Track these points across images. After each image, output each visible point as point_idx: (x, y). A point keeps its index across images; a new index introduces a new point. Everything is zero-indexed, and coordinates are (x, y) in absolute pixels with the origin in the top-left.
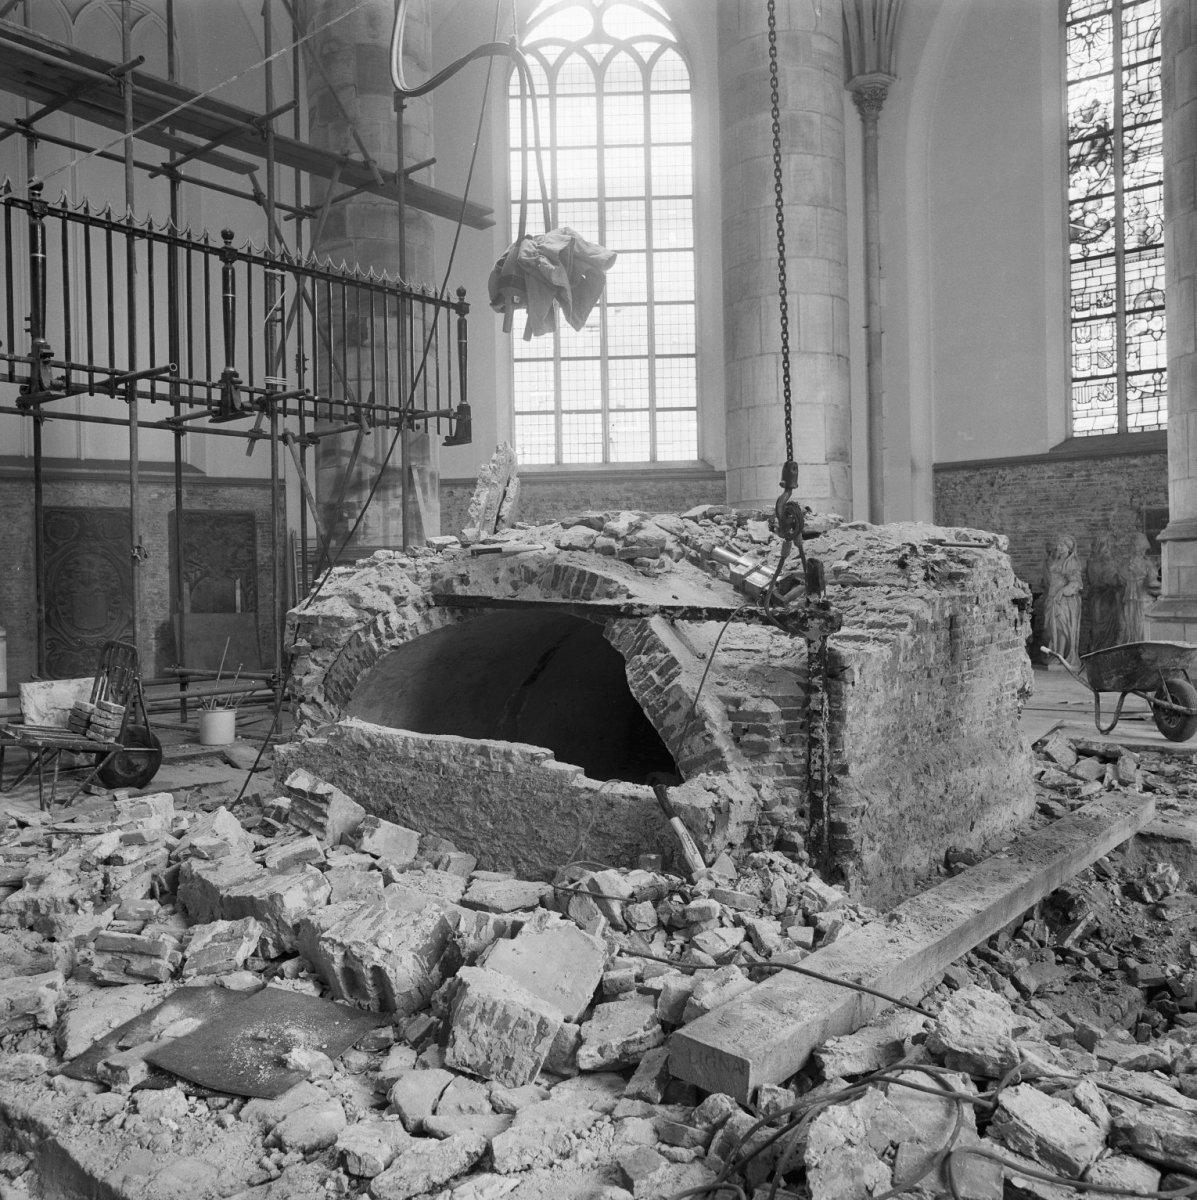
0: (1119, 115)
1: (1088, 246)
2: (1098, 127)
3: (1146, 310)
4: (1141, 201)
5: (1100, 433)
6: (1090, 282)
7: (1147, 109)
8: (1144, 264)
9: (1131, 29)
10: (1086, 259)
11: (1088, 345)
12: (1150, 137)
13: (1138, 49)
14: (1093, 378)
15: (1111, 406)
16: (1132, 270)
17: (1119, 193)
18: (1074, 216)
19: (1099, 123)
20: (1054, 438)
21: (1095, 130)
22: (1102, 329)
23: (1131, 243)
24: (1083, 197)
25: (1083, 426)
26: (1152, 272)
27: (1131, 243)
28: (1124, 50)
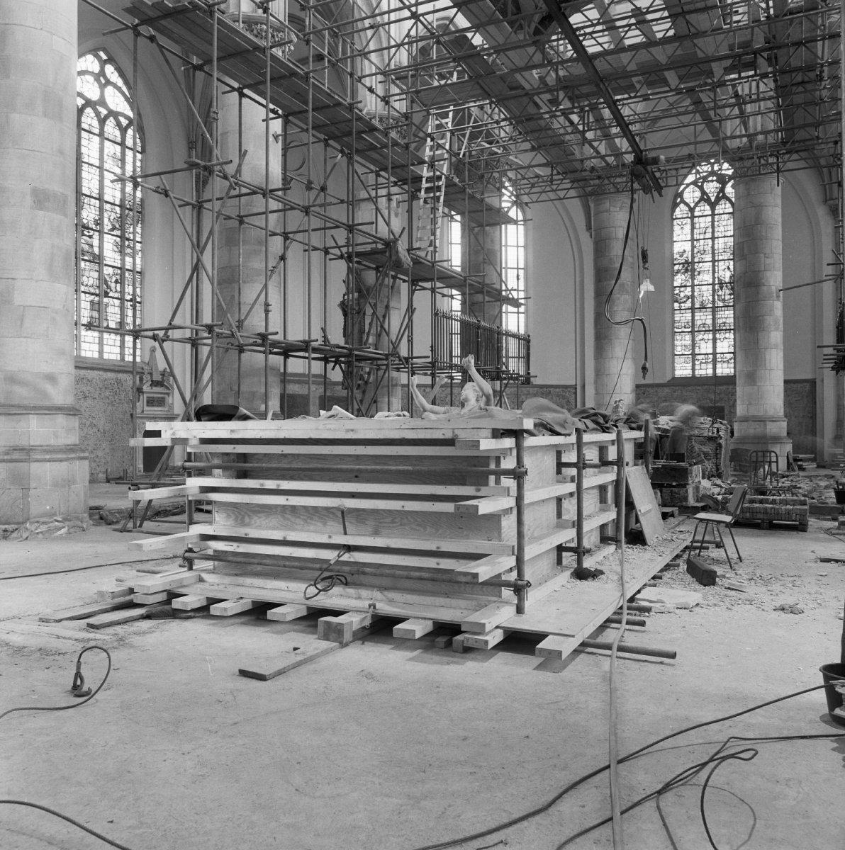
0: (693, 257)
7: (703, 256)
8: (702, 314)
9: (697, 226)
10: (680, 309)
15: (689, 366)
16: (697, 316)
17: (693, 286)
18: (676, 292)
20: (669, 377)
23: (697, 306)
25: (678, 373)
26: (705, 317)
27: (697, 306)
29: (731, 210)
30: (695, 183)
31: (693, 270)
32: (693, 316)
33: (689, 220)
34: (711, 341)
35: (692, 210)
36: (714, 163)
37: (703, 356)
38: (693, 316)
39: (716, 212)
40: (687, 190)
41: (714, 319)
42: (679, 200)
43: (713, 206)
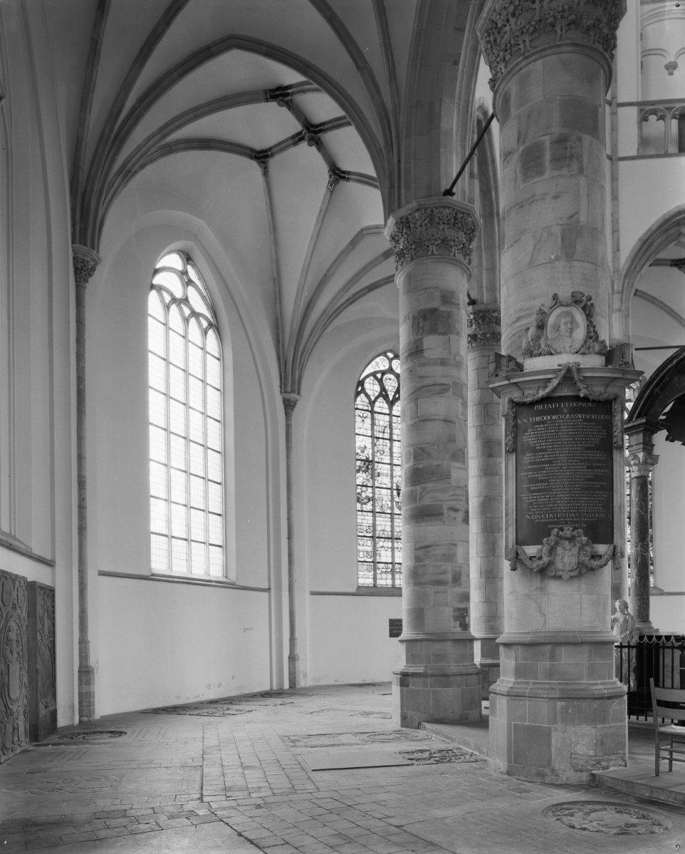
0: (373, 455)
7: (383, 457)
9: (377, 422)
10: (362, 511)
14: (365, 562)
25: (362, 581)
30: (374, 374)
31: (373, 469)
32: (374, 521)
33: (369, 414)
34: (390, 550)
35: (372, 403)
36: (392, 359)
38: (374, 521)
40: (367, 381)
41: (392, 526)
42: (360, 389)
43: (391, 404)
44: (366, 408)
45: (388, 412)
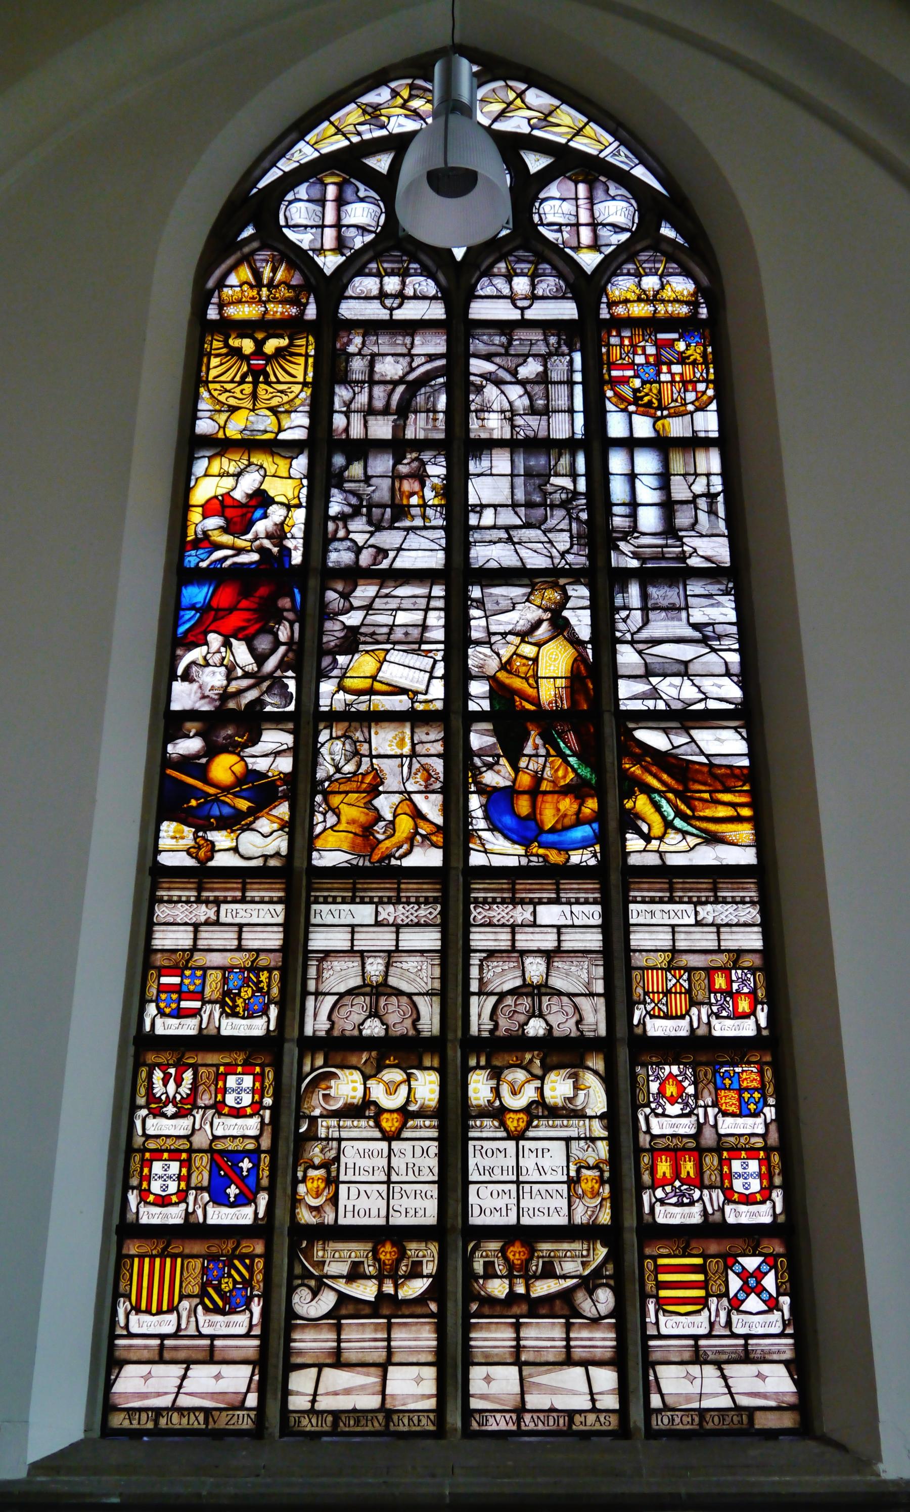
1: (213, 836)
2: (261, 550)
3: (360, 1043)
4: (364, 749)
5: (197, 1422)
6: (209, 938)
7: (389, 539)
8: (364, 913)
11: (181, 1126)
12: (393, 603)
13: (370, 411)
19: (267, 543)
21: (255, 557)
22: (231, 1081)
24: (205, 707)
28: (337, 406)
29: (568, 310)
34: (428, 1129)
37: (358, 1250)
39: (480, 310)
44: (277, 310)
45: (437, 311)
